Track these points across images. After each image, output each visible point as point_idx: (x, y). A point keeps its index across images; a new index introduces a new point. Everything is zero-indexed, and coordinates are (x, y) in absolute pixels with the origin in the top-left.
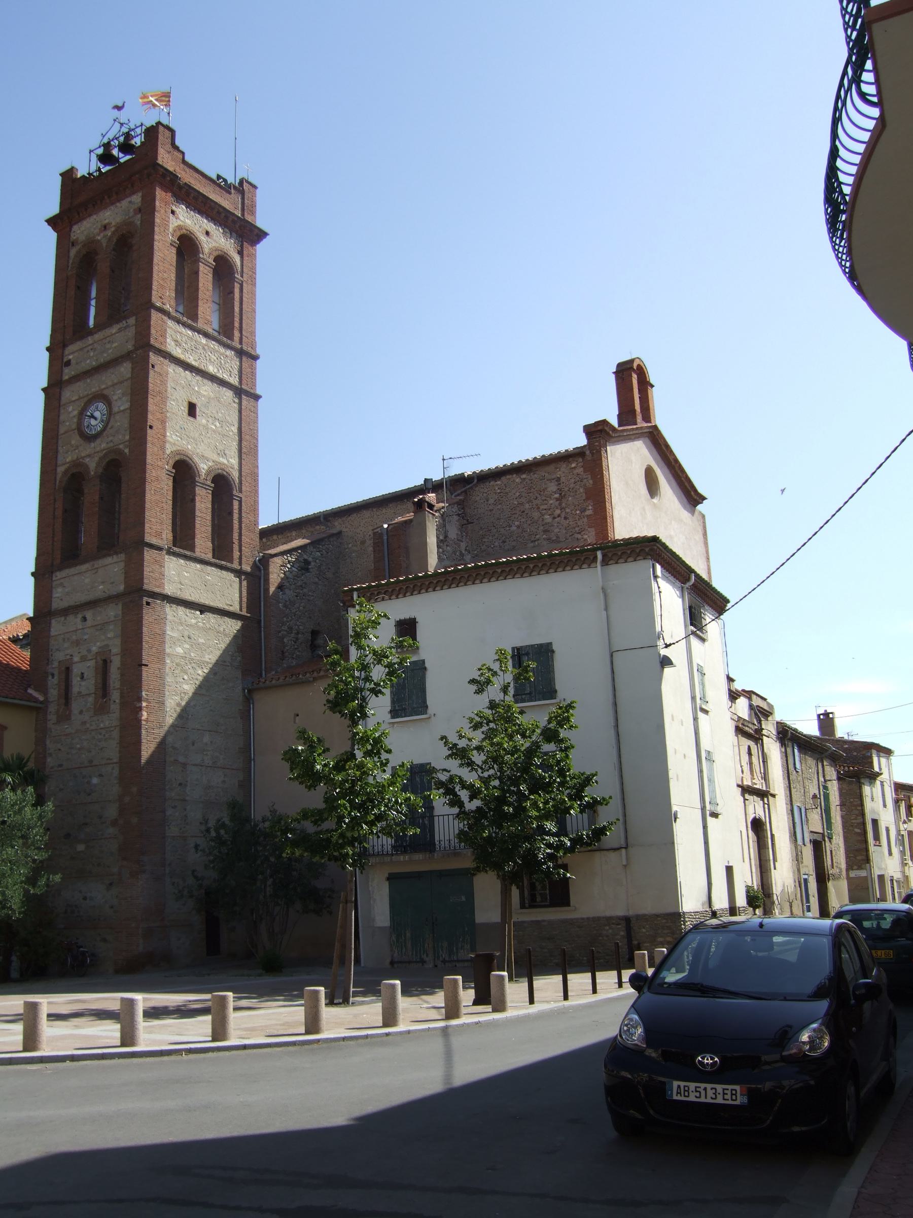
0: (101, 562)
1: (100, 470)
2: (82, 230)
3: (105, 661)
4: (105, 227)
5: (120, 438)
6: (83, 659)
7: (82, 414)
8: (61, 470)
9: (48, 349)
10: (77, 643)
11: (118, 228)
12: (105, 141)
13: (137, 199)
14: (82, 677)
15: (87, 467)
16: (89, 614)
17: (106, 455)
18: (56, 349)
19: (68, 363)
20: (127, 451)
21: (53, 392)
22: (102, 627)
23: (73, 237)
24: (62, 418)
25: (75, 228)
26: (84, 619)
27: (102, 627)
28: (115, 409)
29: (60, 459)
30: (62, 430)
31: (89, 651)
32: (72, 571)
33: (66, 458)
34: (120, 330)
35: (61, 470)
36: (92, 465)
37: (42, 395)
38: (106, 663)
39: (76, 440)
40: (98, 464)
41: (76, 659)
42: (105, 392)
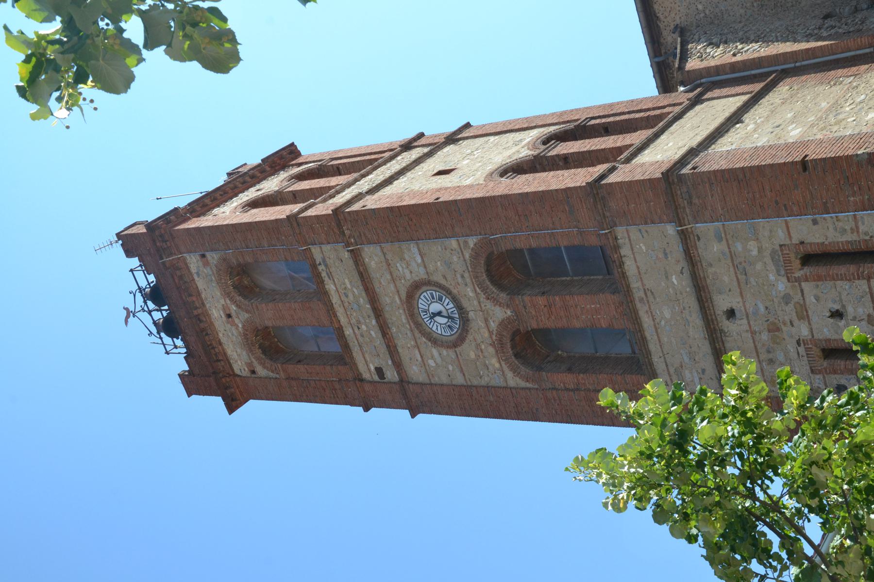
0: (635, 284)
1: (503, 297)
2: (239, 358)
3: (808, 259)
4: (229, 316)
5: (450, 258)
6: (803, 313)
7: (435, 341)
8: (513, 381)
9: (366, 409)
10: (774, 329)
11: (227, 295)
12: (154, 330)
13: (193, 261)
14: (837, 315)
15: (503, 324)
16: (722, 303)
17: (484, 290)
18: (365, 395)
19: (379, 371)
20: (472, 241)
21: (417, 399)
22: (741, 269)
23: (246, 373)
24: (445, 380)
25: (237, 372)
26: (731, 314)
27: (741, 269)
28: (421, 274)
29: (497, 381)
30: (459, 380)
31: (787, 299)
32: (653, 347)
33: (496, 371)
34: (330, 275)
35: (513, 381)
36: (500, 314)
37: (420, 416)
38: (815, 258)
39: (468, 350)
40: (496, 301)
41: (805, 332)
42: (404, 296)
